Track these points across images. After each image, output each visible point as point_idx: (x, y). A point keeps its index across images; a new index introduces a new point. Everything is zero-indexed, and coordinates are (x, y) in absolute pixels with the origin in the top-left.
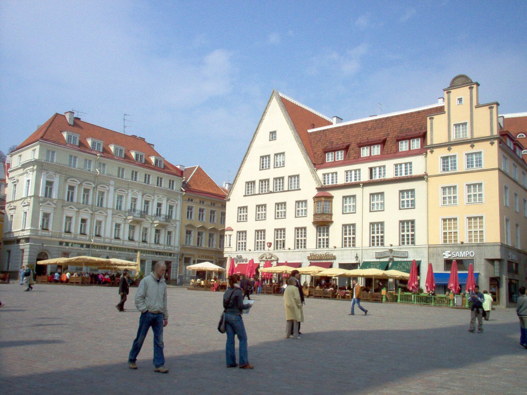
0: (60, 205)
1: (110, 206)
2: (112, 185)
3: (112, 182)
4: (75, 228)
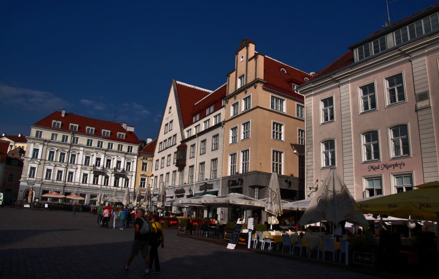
0: (42, 162)
1: (80, 162)
2: (82, 151)
3: (82, 149)
4: (54, 176)
